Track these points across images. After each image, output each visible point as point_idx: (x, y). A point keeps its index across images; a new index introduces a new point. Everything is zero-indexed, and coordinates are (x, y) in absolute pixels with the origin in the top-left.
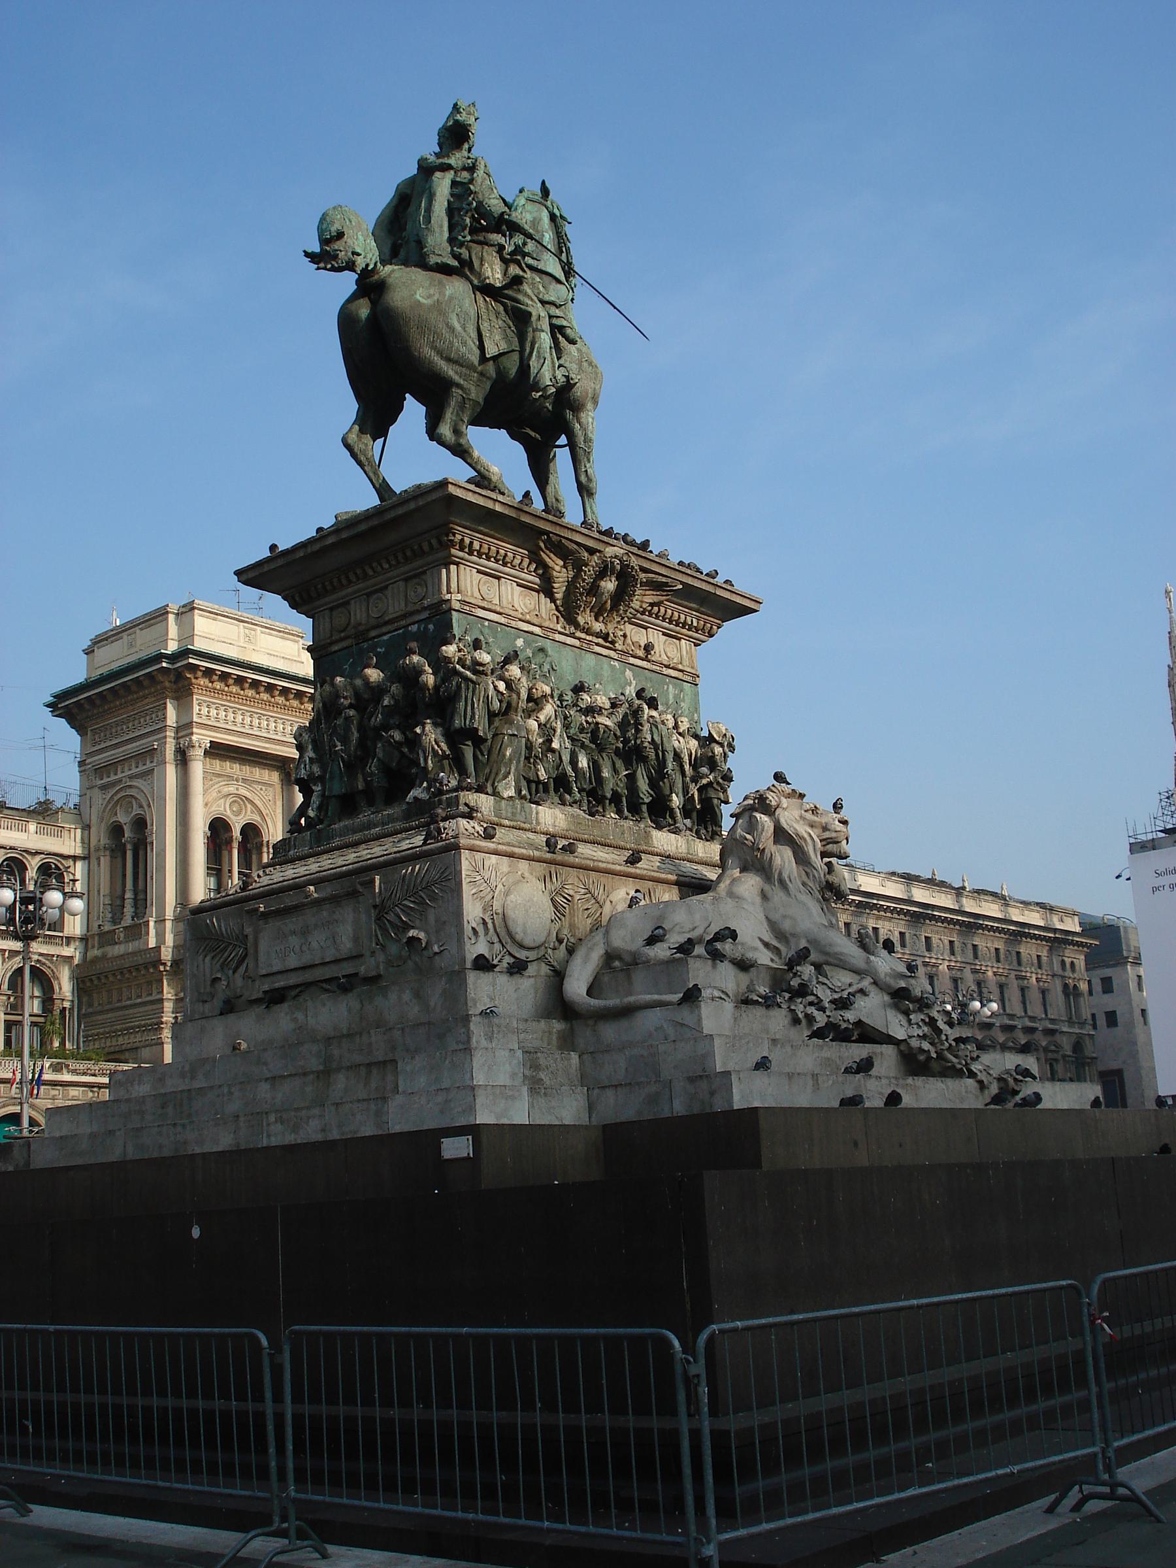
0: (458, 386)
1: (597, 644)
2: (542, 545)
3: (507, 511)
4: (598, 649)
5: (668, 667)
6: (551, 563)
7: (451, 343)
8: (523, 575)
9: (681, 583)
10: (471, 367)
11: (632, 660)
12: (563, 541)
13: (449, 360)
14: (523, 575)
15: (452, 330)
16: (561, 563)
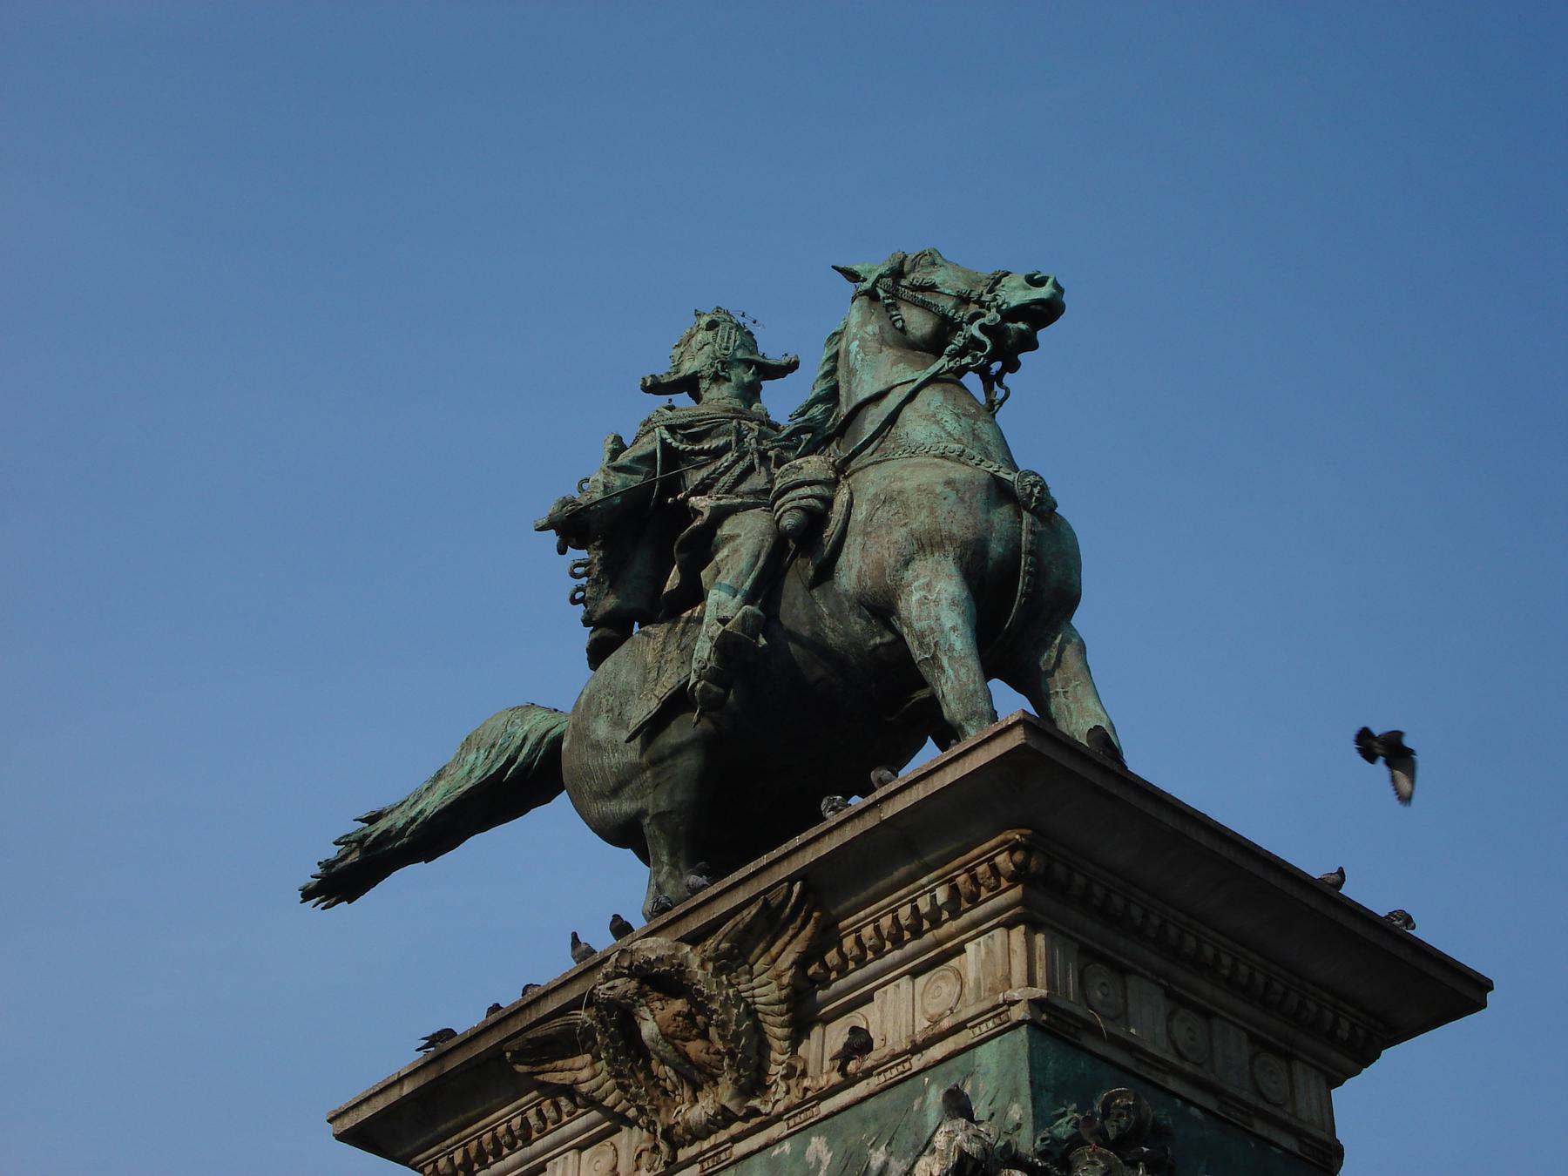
0: (642, 813)
1: (735, 1139)
2: (520, 1068)
3: (419, 1081)
4: (741, 1148)
5: (917, 1048)
6: (567, 1078)
7: (602, 768)
8: (567, 1130)
9: (791, 879)
10: (635, 770)
11: (827, 1106)
12: (530, 1035)
13: (615, 792)
14: (567, 1130)
15: (597, 747)
16: (588, 1057)
